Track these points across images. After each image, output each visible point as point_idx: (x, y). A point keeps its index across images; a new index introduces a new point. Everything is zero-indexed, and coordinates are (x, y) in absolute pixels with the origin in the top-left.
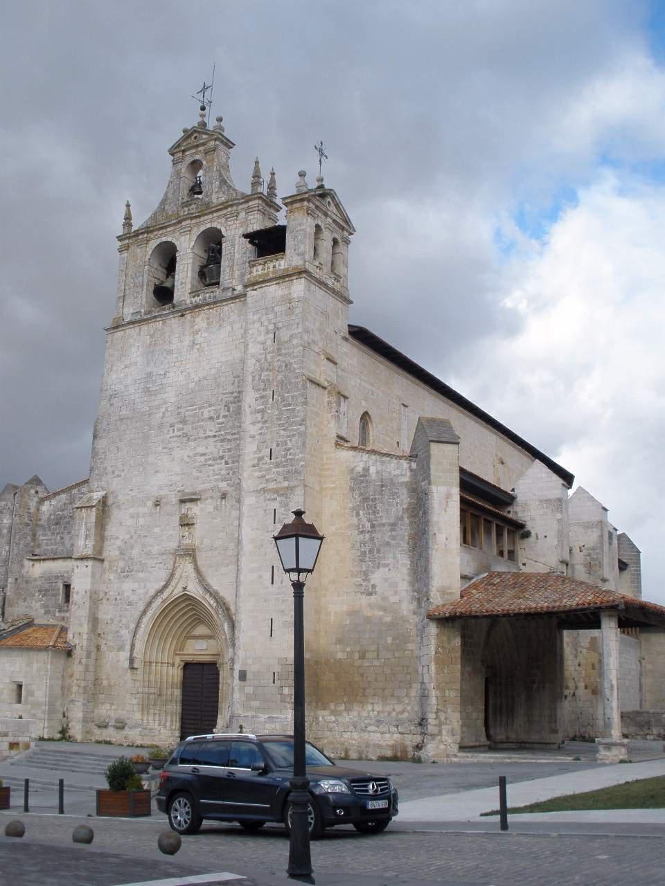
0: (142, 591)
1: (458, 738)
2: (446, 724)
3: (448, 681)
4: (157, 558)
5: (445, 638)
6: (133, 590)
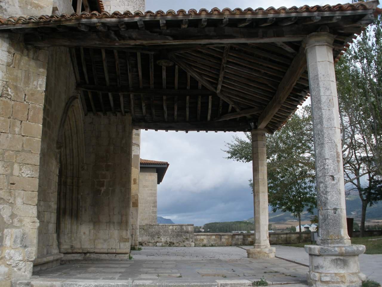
1: (32, 251)
2: (12, 226)
3: (19, 147)
5: (20, 74)
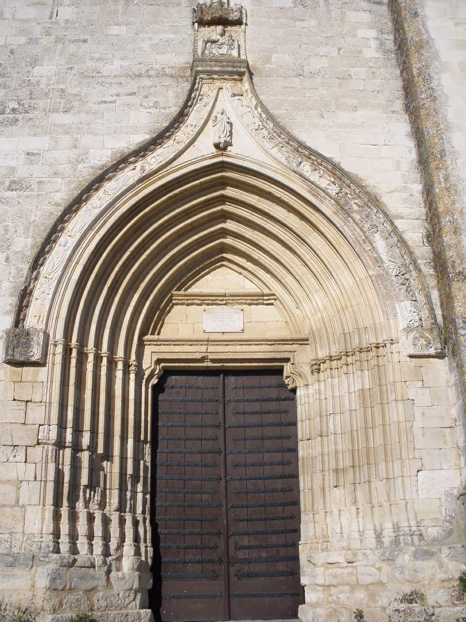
0: (63, 154)
4: (121, 83)
6: (28, 154)
